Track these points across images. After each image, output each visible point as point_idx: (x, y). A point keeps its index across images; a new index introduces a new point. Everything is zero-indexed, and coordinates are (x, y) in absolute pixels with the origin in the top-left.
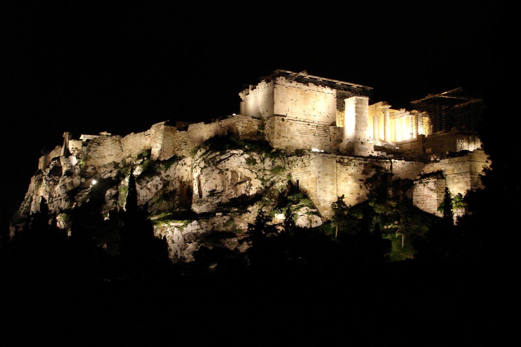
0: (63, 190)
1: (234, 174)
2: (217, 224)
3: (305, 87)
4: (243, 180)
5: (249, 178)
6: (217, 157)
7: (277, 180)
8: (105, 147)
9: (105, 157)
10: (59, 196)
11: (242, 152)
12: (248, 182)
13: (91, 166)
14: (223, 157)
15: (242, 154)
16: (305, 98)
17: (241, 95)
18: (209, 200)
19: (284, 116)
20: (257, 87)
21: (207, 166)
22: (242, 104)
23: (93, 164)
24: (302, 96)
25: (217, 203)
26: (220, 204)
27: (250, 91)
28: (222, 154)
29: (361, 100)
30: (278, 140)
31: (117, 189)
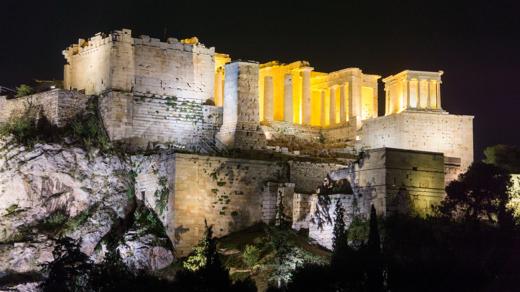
1: (47, 181)
2: (16, 260)
3: (164, 45)
4: (60, 191)
5: (69, 188)
6: (21, 155)
11: (59, 147)
12: (68, 194)
14: (29, 155)
15: (61, 151)
16: (163, 62)
17: (64, 53)
18: (6, 222)
21: (5, 168)
22: (67, 68)
24: (159, 59)
25: (18, 228)
26: (22, 229)
27: (80, 49)
28: (27, 150)
29: (248, 67)
30: (117, 129)
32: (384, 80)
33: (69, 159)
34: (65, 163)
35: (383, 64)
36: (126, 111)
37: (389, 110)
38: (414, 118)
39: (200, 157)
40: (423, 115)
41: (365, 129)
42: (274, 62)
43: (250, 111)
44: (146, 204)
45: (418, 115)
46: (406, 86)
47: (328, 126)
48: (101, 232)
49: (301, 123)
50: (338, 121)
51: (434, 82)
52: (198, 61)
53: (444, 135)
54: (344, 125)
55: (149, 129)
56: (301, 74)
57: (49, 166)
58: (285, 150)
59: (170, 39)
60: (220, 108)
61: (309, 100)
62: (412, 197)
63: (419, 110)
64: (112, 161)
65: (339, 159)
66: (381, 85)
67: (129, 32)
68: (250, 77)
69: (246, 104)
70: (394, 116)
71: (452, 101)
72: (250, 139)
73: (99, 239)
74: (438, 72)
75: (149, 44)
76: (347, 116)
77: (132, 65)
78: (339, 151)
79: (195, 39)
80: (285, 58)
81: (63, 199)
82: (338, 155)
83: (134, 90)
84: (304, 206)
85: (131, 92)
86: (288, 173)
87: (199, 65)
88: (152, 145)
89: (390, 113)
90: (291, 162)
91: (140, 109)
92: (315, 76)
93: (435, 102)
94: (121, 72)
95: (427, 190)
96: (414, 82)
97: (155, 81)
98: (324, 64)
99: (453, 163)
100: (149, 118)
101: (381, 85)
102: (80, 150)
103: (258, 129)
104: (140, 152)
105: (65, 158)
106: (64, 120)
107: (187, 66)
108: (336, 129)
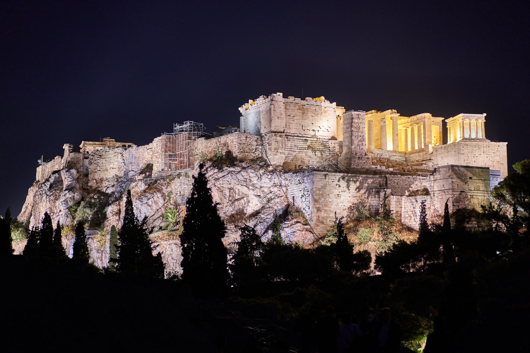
0: (64, 205)
1: (232, 191)
3: (303, 102)
6: (215, 174)
7: (273, 197)
8: (107, 159)
9: (107, 170)
10: (60, 211)
12: (245, 199)
13: (93, 179)
16: (303, 113)
17: (240, 109)
19: (281, 132)
20: (256, 102)
23: (96, 177)
24: (301, 111)
29: (358, 115)
31: (119, 205)
32: (446, 121)
33: (246, 177)
34: (243, 179)
35: (445, 109)
36: (280, 145)
37: (450, 140)
38: (467, 145)
39: (329, 174)
40: (474, 143)
41: (435, 153)
42: (373, 111)
43: (360, 143)
44: (295, 204)
45: (470, 142)
46: (462, 124)
47: (410, 152)
48: (267, 223)
49: (392, 150)
50: (416, 148)
51: (480, 121)
52: (325, 112)
53: (488, 156)
54: (421, 150)
55: (295, 156)
56: (391, 118)
57: (233, 181)
58: (384, 168)
59: (307, 98)
60: (340, 141)
61: (397, 135)
62: (469, 197)
63: (470, 139)
64: (273, 177)
65: (419, 173)
66: (444, 124)
67: (281, 94)
68: (360, 121)
69: (357, 139)
70: (454, 144)
71: (493, 133)
72: (361, 161)
73: (266, 227)
74: (482, 114)
75: (294, 102)
76: (423, 144)
77: (283, 116)
78: (418, 167)
79: (323, 98)
80: (381, 109)
81: (242, 201)
82: (417, 170)
83: (285, 131)
84: (398, 204)
85: (284, 132)
86: (386, 183)
87: (326, 114)
88: (297, 166)
89: (452, 142)
90: (388, 176)
91: (289, 144)
92: (400, 119)
93: (481, 134)
94: (277, 120)
95: (479, 192)
96: (467, 121)
97: (298, 125)
98: (406, 111)
99: (496, 175)
100: (295, 149)
101: (444, 124)
102: (253, 171)
103: (366, 154)
104: (290, 171)
105: (243, 176)
106: (242, 152)
107: (319, 115)
108: (416, 153)
